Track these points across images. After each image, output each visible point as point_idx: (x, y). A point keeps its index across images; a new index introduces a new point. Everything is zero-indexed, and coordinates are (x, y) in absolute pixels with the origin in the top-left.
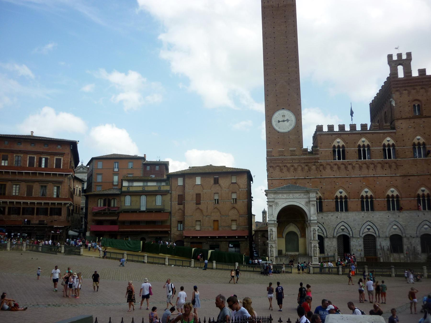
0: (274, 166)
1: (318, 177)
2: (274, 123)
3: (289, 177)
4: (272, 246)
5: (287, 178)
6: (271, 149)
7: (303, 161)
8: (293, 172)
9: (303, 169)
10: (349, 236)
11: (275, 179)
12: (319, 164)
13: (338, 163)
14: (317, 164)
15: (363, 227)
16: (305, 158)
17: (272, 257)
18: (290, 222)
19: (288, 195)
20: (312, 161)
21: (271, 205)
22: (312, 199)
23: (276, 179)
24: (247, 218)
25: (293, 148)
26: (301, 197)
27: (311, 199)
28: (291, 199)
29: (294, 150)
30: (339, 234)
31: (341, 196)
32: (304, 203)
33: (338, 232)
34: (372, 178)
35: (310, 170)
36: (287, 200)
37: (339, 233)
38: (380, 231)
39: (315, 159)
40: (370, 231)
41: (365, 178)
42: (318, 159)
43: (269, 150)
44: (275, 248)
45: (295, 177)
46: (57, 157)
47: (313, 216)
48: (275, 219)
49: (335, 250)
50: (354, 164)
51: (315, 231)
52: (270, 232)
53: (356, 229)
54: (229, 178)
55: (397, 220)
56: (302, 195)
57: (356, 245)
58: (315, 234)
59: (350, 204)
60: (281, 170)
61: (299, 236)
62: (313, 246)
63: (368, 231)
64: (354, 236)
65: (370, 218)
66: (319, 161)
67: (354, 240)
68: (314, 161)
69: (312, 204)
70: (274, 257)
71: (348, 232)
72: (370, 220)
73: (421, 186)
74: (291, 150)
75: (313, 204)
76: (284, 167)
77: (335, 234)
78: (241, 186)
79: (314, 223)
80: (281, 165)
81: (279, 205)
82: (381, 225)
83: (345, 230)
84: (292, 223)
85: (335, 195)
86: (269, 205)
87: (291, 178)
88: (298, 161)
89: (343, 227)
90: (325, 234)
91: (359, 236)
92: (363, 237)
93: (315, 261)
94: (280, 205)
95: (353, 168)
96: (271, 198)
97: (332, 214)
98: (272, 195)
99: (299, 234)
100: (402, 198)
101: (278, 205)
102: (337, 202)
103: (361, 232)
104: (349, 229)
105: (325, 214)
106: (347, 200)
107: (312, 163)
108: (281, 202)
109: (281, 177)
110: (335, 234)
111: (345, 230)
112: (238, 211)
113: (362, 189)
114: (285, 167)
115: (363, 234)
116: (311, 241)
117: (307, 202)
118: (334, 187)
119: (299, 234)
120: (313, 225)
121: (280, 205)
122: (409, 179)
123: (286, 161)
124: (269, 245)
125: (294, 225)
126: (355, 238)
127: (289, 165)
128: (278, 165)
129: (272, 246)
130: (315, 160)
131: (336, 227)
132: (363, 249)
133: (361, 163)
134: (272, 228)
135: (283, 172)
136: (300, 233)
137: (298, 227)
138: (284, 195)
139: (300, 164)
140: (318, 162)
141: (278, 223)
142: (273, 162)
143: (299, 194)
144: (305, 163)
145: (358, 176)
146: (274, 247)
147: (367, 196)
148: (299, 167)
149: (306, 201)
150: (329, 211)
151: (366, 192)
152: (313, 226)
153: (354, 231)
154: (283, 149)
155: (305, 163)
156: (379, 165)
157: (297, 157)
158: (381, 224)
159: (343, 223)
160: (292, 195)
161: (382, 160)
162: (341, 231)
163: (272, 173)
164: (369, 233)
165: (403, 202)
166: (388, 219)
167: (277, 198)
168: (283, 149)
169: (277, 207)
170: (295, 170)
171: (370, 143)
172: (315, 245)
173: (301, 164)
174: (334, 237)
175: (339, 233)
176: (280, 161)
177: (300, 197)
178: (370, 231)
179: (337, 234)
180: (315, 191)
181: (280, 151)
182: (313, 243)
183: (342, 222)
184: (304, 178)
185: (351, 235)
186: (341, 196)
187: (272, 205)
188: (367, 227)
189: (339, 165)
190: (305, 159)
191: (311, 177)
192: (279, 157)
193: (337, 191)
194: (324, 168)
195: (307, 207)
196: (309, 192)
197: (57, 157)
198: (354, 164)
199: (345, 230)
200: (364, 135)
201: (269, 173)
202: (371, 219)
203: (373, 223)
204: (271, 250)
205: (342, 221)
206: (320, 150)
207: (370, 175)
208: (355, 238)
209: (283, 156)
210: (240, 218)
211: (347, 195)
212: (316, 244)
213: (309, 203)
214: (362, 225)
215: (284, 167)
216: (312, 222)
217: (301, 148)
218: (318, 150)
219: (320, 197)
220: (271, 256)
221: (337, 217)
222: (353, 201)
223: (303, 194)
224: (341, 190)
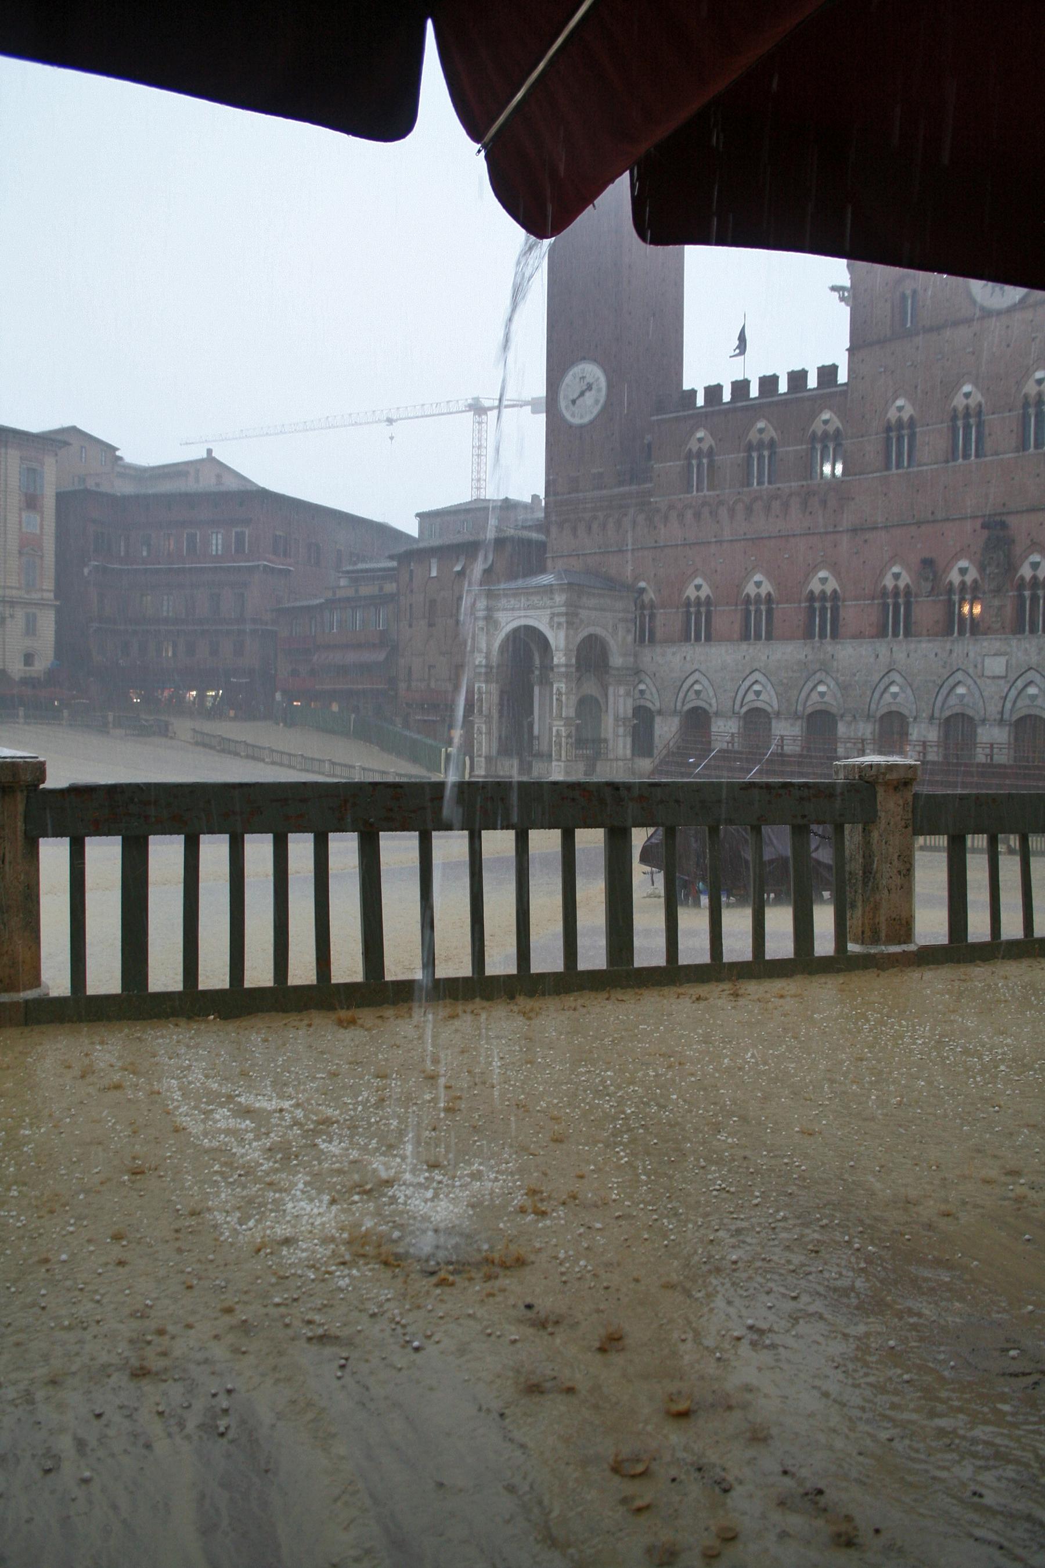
2: (563, 404)
31: (698, 598)
32: (548, 620)
33: (688, 699)
36: (517, 614)
46: (238, 529)
73: (893, 560)
77: (679, 704)
90: (658, 704)
95: (732, 511)
100: (844, 600)
102: (688, 614)
105: (658, 650)
110: (679, 704)
113: (748, 574)
115: (742, 706)
122: (866, 541)
124: (476, 726)
146: (484, 730)
150: (669, 641)
161: (800, 483)
162: (693, 696)
164: (758, 704)
165: (849, 613)
174: (675, 712)
179: (683, 704)
186: (698, 598)
194: (666, 519)
197: (238, 529)
219: (651, 600)
221: (685, 658)
224: (699, 581)
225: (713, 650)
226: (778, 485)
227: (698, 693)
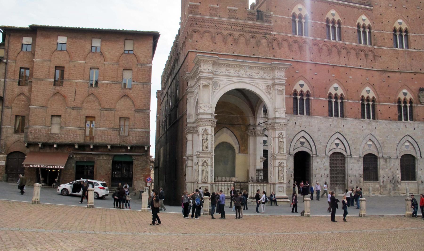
0: (202, 30)
1: (269, 58)
3: (224, 52)
4: (205, 162)
5: (221, 53)
6: (197, 2)
7: (249, 29)
8: (232, 45)
9: (247, 42)
10: (311, 153)
11: (201, 51)
12: (271, 37)
13: (299, 40)
14: (268, 37)
15: (330, 140)
16: (252, 25)
17: (206, 183)
18: (224, 127)
19: (238, 69)
20: (262, 31)
21: (206, 84)
22: (279, 80)
23: (203, 52)
25: (233, 6)
26: (259, 76)
27: (277, 81)
28: (242, 77)
29: (235, 10)
30: (296, 150)
31: (302, 91)
32: (264, 87)
34: (343, 68)
35: (258, 44)
36: (236, 79)
37: (296, 148)
38: (352, 148)
39: (265, 28)
40: (338, 147)
41: (335, 67)
42: (271, 29)
43: (195, 3)
45: (234, 53)
48: (213, 111)
49: (290, 176)
50: (322, 45)
51: (283, 138)
52: (203, 135)
53: (320, 143)
54: (119, 43)
55: (373, 133)
56: (262, 73)
57: (320, 168)
59: (314, 105)
60: (213, 39)
61: (237, 150)
62: (277, 165)
63: (337, 147)
64: (318, 154)
65: (340, 128)
66: (272, 33)
67: (318, 160)
68: (265, 31)
69: (277, 89)
70: (209, 184)
71: (310, 148)
72: (340, 131)
73: (402, 88)
74: (229, 9)
75: (280, 91)
76: (218, 35)
77: (292, 149)
78: (140, 58)
79: (281, 123)
80: (212, 30)
81: (219, 87)
82: (353, 139)
83: (306, 144)
84: (227, 128)
85: (293, 88)
86: (204, 84)
87: (228, 54)
88: (240, 28)
89: (303, 140)
91: (324, 155)
92: (329, 155)
93: (280, 191)
94: (223, 88)
96: (209, 71)
97: (289, 118)
98: (209, 66)
99: (236, 147)
100: (379, 102)
101: (218, 87)
103: (328, 149)
104: (312, 144)
106: (310, 98)
107: (261, 33)
108: (224, 82)
109: (212, 51)
110: (292, 149)
111: (306, 144)
112: (133, 103)
113: (330, 82)
114: (219, 35)
117: (268, 86)
118: (293, 76)
119: (236, 147)
120: (278, 127)
121: (223, 88)
122: (389, 77)
123: (222, 26)
125: (229, 132)
126: (319, 156)
127: (225, 33)
128: (208, 30)
129: (206, 163)
130: (266, 30)
131: (293, 139)
132: (329, 174)
133: (330, 45)
134: (207, 128)
135: (215, 43)
136: (238, 146)
137: (235, 135)
138: (231, 69)
139: (242, 33)
140: (271, 34)
141: (216, 120)
142: (200, 23)
143: (257, 71)
144: (250, 32)
145: (326, 64)
147: (336, 94)
148: (242, 38)
149: (268, 85)
151: (336, 89)
152: (280, 129)
153: (318, 146)
154: (217, 5)
155: (250, 32)
156: (353, 52)
157: (238, 21)
158: (353, 137)
159: (303, 134)
160: (245, 72)
161: (356, 44)
162: (300, 145)
163: (197, 41)
164: (338, 150)
165: (381, 108)
166: (363, 130)
167: (218, 73)
168: (218, 6)
169: (217, 91)
170: (236, 41)
171: (341, 19)
173: (245, 33)
175: (296, 148)
176: (211, 25)
177: (257, 76)
178: (338, 147)
179: (294, 150)
180: (284, 68)
181: (211, 9)
182: (278, 159)
183: (301, 131)
184: (248, 56)
185: (314, 153)
187: (208, 85)
188: (335, 140)
189: (301, 43)
190: (251, 27)
191: (259, 57)
192: (210, 17)
193: (297, 82)
195: (268, 95)
196: (275, 67)
198: (321, 45)
199: (305, 144)
200: (335, 5)
201: (192, 41)
202: (341, 129)
203: (343, 135)
204: (203, 171)
205: (302, 130)
206: (274, 15)
207: (341, 65)
208: (319, 156)
209: (216, 16)
210: (137, 115)
211: (310, 90)
213: (272, 88)
214: (330, 137)
215: (218, 35)
216: (277, 121)
217: (246, 8)
218: (270, 16)
220: (204, 181)
221: (295, 123)
222: (318, 100)
223: (263, 72)
224: (302, 82)
225: (313, 120)
226: (345, 42)
227: (302, 143)
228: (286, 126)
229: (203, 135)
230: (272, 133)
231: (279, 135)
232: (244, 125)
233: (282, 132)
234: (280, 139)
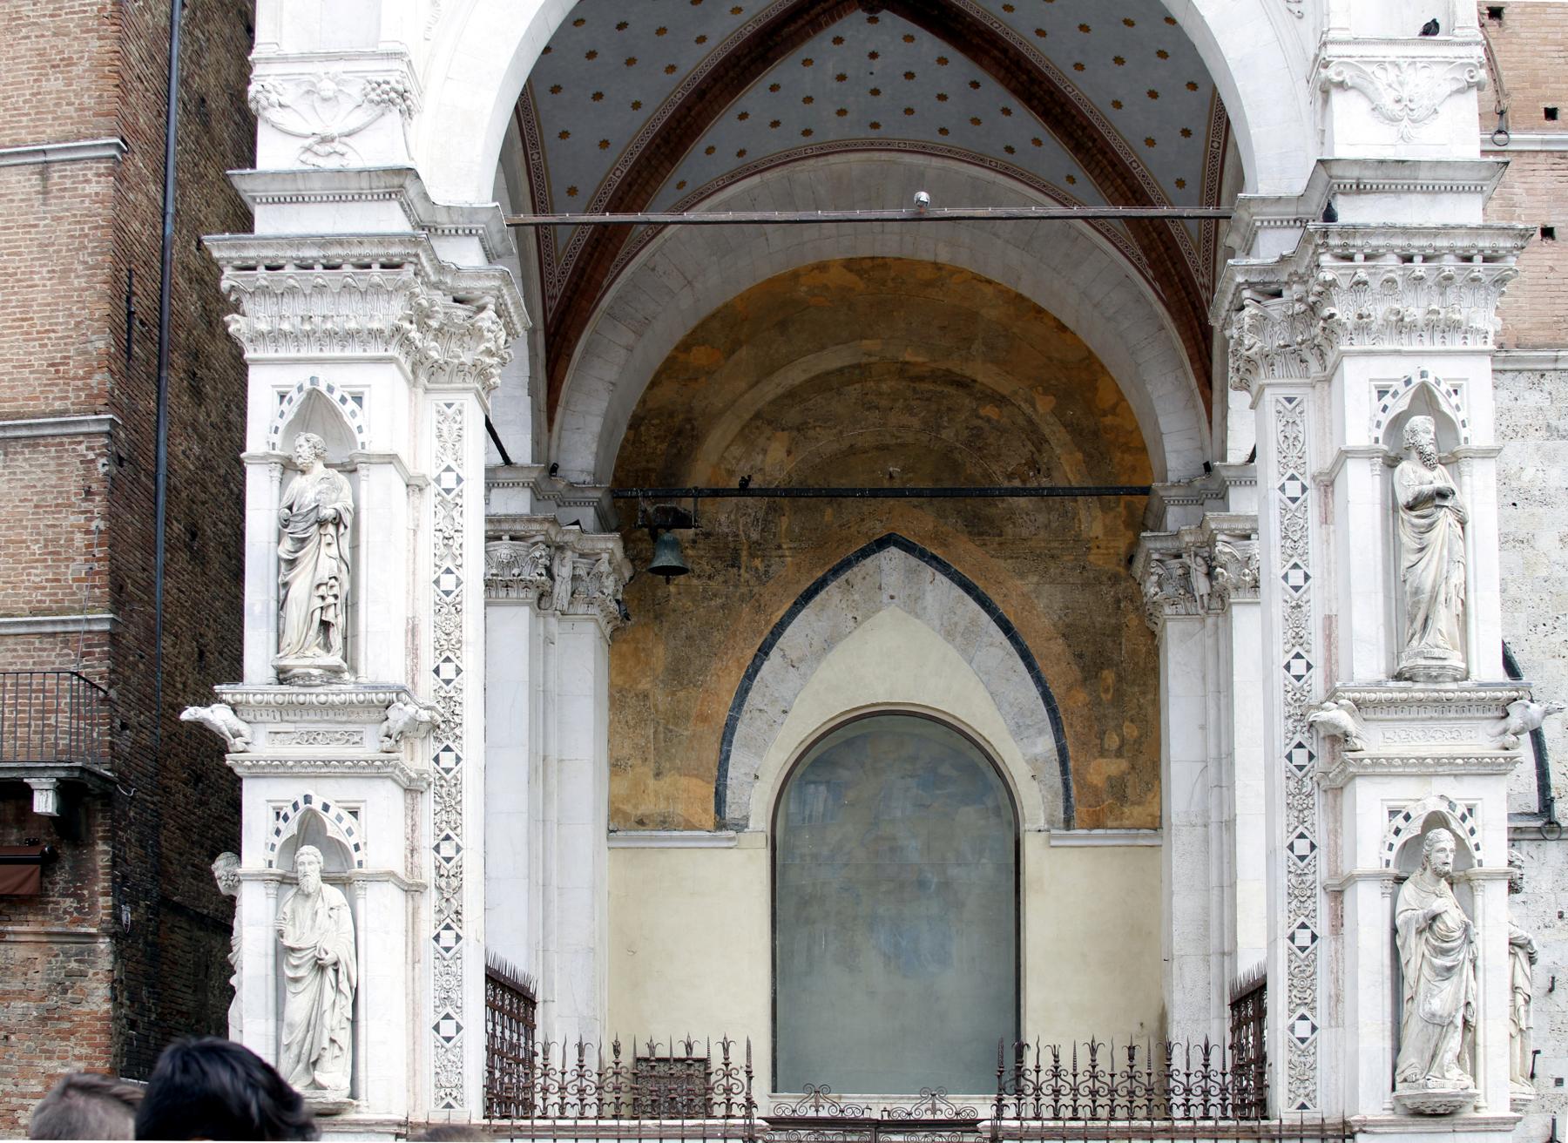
24: (101, 467)
44: (413, 890)
47: (1383, 78)
52: (289, 467)
58: (1445, 519)
116: (1341, 717)
120: (1379, 310)
152: (1400, 325)
172: (1436, 820)
212: (1462, 791)
228: (1502, 281)
229: (289, 467)
230: (1310, 407)
231: (1398, 422)
232: (1116, 491)
233: (1441, 371)
234: (1413, 478)
